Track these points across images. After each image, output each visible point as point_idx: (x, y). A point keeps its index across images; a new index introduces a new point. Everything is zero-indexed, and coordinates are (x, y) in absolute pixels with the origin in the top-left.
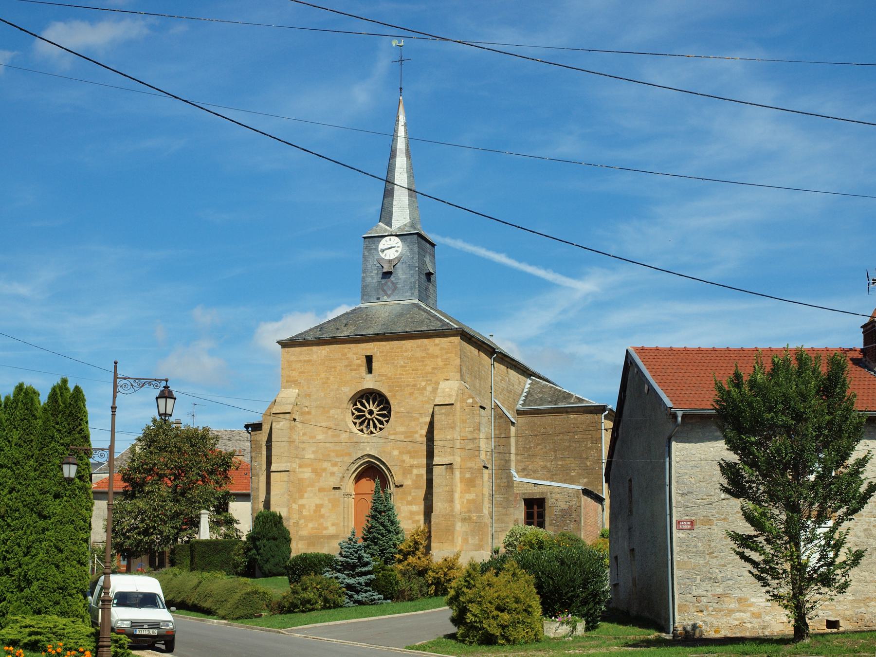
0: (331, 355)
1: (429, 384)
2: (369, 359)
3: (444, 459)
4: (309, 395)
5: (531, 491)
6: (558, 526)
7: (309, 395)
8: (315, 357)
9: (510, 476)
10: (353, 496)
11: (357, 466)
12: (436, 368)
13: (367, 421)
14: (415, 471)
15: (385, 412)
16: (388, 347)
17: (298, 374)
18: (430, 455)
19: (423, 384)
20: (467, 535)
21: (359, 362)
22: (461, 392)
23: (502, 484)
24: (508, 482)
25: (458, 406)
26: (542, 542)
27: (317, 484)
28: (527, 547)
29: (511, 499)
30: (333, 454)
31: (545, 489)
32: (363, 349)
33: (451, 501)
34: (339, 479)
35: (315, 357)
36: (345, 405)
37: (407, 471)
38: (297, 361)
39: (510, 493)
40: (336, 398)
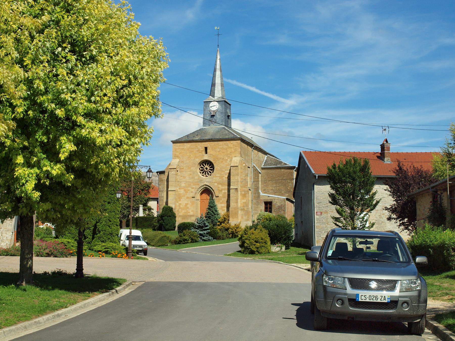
2: (206, 148)
4: (183, 162)
6: (277, 212)
7: (183, 162)
8: (185, 147)
9: (259, 193)
14: (223, 191)
15: (212, 169)
17: (179, 153)
18: (229, 185)
19: (227, 158)
21: (202, 149)
22: (241, 162)
23: (256, 196)
24: (258, 195)
25: (240, 167)
26: (271, 218)
27: (186, 196)
28: (265, 220)
29: (259, 202)
31: (272, 198)
33: (237, 202)
35: (185, 147)
36: (197, 166)
37: (220, 191)
38: (178, 149)
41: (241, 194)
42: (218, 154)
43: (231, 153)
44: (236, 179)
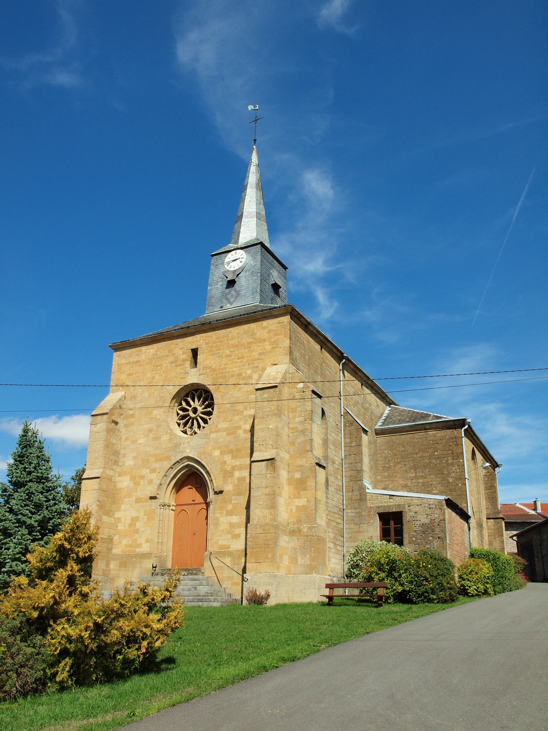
0: (158, 353)
1: (256, 372)
2: (195, 352)
3: (265, 454)
5: (386, 504)
6: (418, 544)
8: (143, 357)
9: (362, 488)
10: (174, 508)
11: (176, 471)
12: (263, 353)
13: (191, 420)
14: (237, 474)
16: (214, 337)
17: (126, 376)
19: (249, 372)
20: (296, 552)
21: (184, 356)
23: (354, 498)
24: (360, 495)
26: (394, 562)
27: (134, 493)
28: (375, 569)
29: (364, 513)
30: (152, 459)
32: (189, 343)
33: (273, 506)
34: (156, 487)
35: (143, 357)
37: (228, 474)
38: (127, 363)
39: (363, 507)
40: (160, 397)
41: (290, 481)
42: (225, 365)
43: (263, 357)
44: (271, 427)
